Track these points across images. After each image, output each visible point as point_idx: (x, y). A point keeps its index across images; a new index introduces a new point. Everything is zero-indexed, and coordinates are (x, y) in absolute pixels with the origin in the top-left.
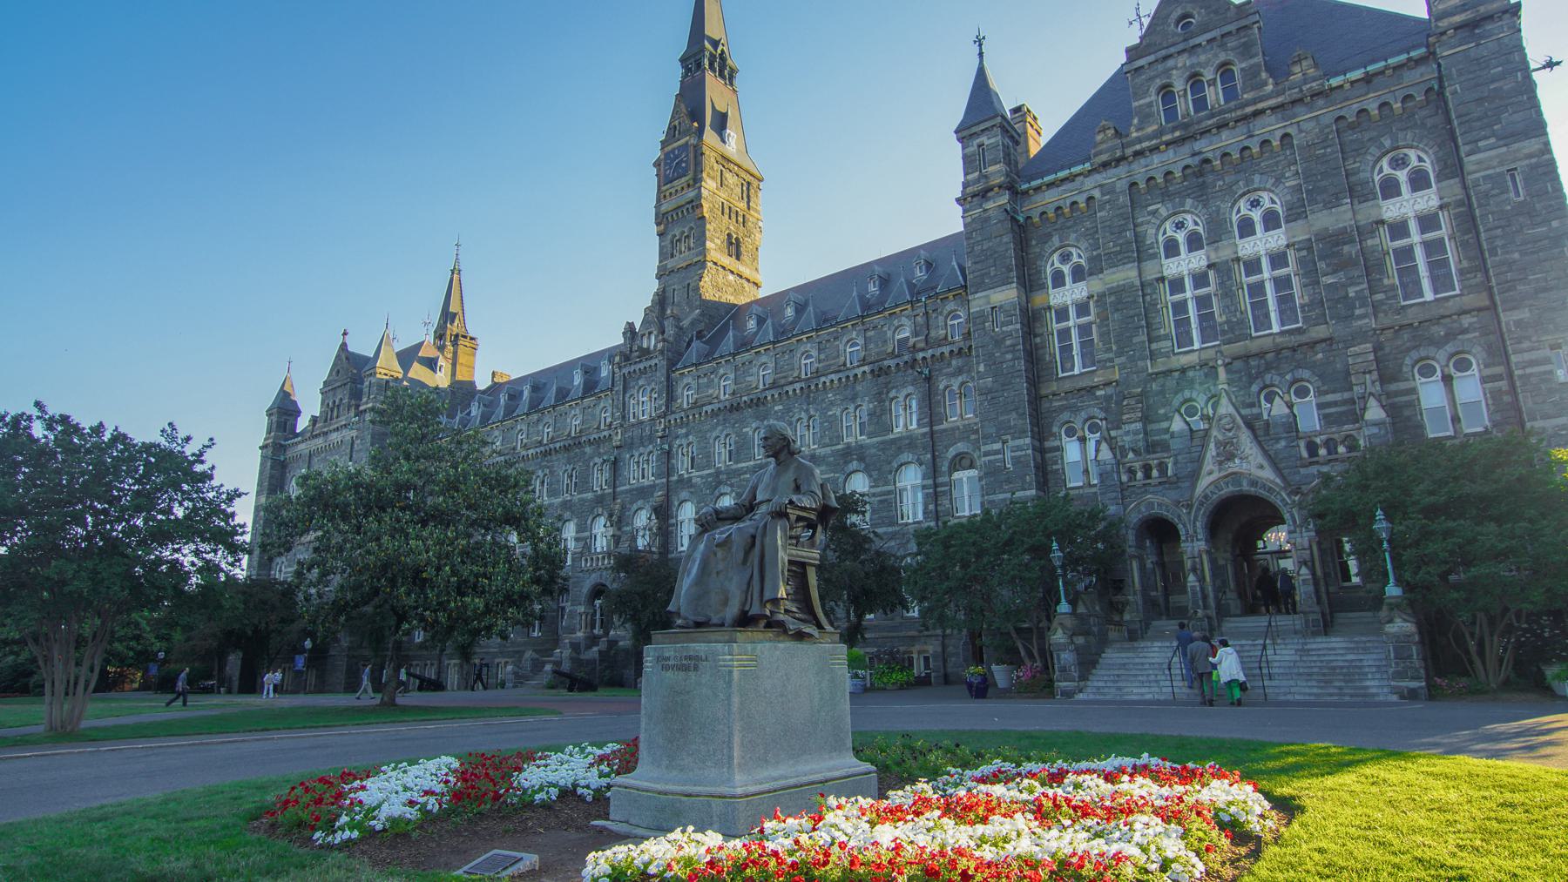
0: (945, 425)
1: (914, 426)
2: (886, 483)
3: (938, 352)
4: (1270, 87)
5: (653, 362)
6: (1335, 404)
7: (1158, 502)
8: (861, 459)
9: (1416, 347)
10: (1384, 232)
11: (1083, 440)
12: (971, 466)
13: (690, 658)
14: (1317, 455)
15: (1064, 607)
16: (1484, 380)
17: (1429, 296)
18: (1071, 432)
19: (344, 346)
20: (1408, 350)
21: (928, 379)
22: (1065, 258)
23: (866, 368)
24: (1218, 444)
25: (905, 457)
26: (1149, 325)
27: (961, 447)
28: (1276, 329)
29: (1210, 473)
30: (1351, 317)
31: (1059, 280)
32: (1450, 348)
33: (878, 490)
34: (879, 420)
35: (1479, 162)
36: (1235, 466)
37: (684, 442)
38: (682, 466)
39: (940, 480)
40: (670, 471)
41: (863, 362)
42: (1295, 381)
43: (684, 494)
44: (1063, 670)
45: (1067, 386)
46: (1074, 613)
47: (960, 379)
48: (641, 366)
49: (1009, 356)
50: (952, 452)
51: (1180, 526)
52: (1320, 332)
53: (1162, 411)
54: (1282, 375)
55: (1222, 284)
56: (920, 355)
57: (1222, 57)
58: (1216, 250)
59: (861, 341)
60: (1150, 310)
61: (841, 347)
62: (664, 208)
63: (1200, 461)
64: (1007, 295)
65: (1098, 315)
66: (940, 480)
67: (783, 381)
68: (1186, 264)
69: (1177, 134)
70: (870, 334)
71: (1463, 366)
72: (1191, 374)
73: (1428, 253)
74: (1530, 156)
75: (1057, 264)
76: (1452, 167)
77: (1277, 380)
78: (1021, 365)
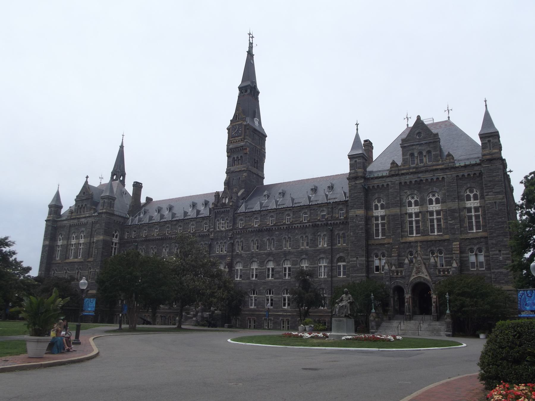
0: (336, 247)
1: (326, 246)
2: (315, 264)
3: (336, 222)
4: (440, 162)
5: (228, 209)
7: (400, 282)
8: (307, 254)
10: (466, 211)
12: (344, 261)
15: (373, 311)
16: (485, 256)
17: (475, 231)
18: (377, 256)
19: (86, 182)
21: (332, 230)
22: (379, 202)
23: (311, 224)
24: (416, 268)
25: (322, 256)
26: (402, 227)
27: (341, 254)
28: (436, 234)
29: (414, 276)
30: (454, 234)
31: (377, 208)
32: (477, 246)
33: (312, 266)
34: (314, 242)
35: (488, 198)
36: (421, 275)
37: (239, 240)
38: (238, 250)
39: (333, 265)
40: (233, 251)
41: (309, 222)
42: (439, 250)
43: (238, 260)
45: (377, 242)
46: (375, 312)
47: (342, 232)
48: (223, 210)
49: (360, 232)
50: (338, 256)
52: (447, 237)
54: (436, 248)
55: (422, 218)
56: (329, 222)
57: (429, 149)
58: (422, 207)
59: (309, 213)
60: (402, 223)
61: (301, 214)
62: (231, 146)
63: (411, 272)
64: (361, 212)
65: (387, 221)
66: (333, 265)
67: (279, 224)
68: (413, 209)
69: (414, 170)
70: (312, 211)
71: (480, 251)
72: (412, 244)
73: (476, 219)
74: (500, 199)
75: (376, 203)
76: (482, 197)
78: (364, 235)
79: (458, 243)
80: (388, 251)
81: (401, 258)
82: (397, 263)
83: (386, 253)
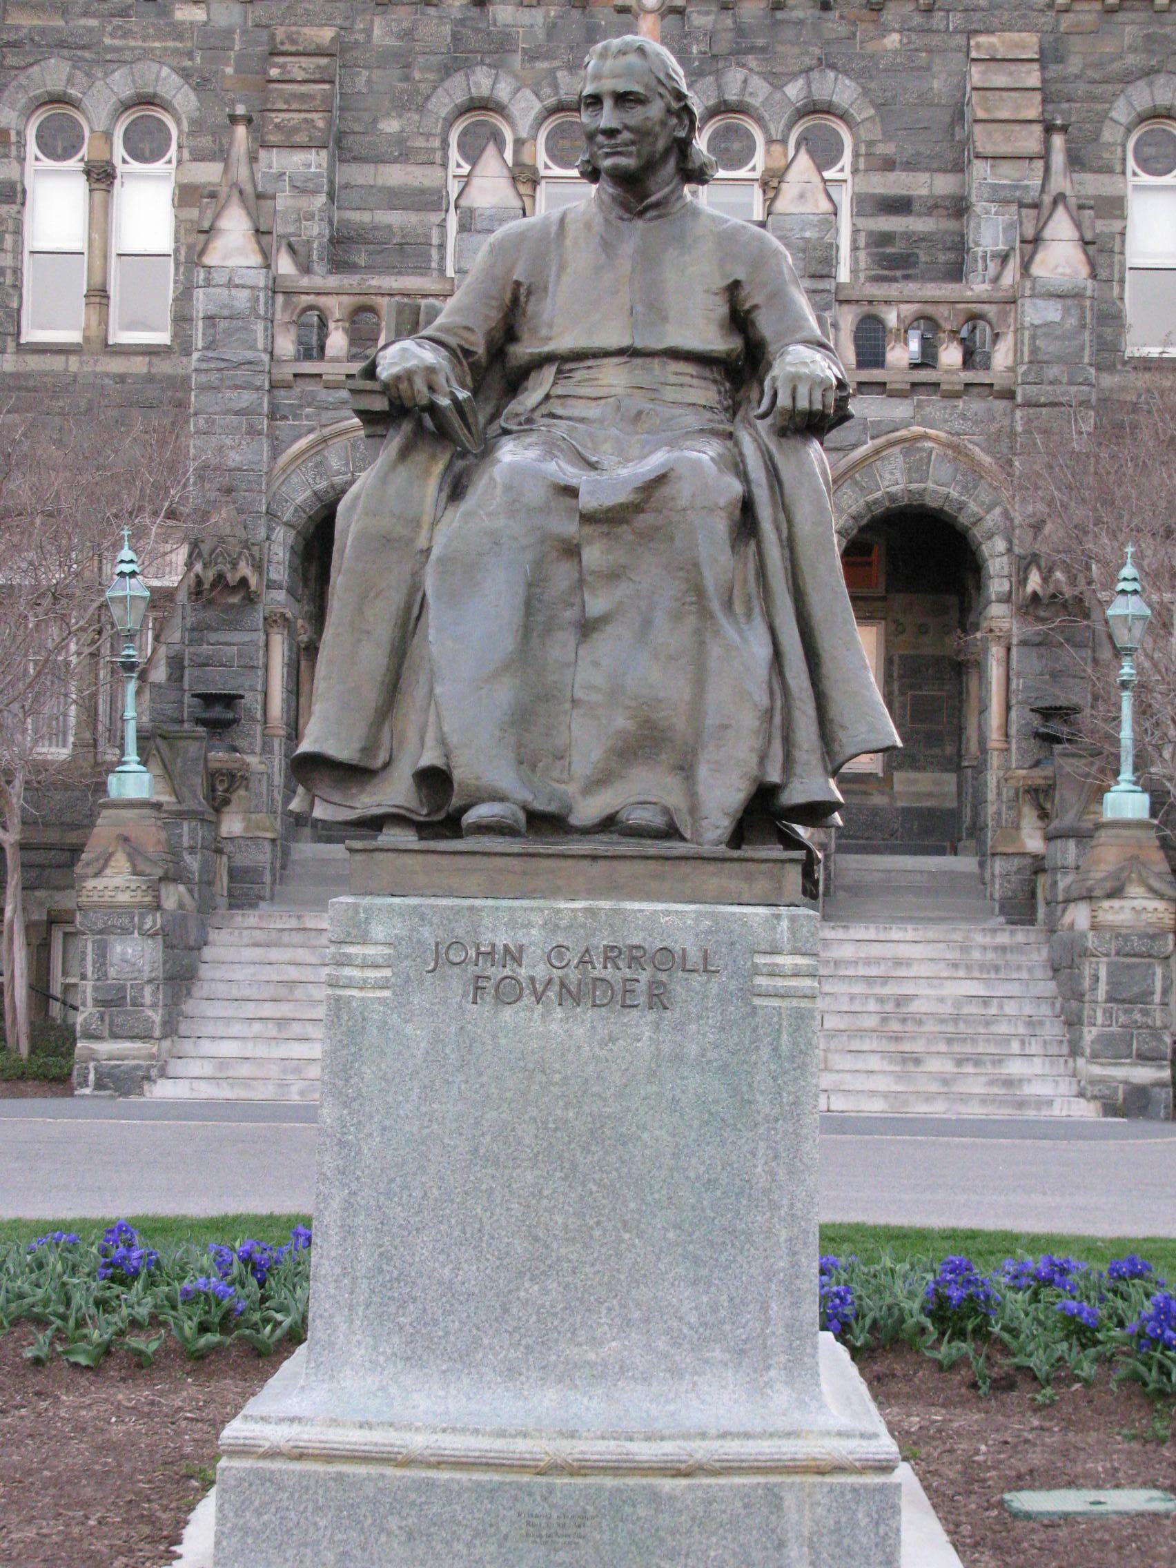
9: (1149, 73)
11: (101, 176)
13: (636, 956)
18: (60, 142)
20: (1127, 78)
42: (813, 108)
53: (391, 126)
54: (776, 80)
77: (759, 91)
79: (1029, 44)
80: (202, 84)
81: (360, 174)
82: (316, 230)
83: (185, 99)
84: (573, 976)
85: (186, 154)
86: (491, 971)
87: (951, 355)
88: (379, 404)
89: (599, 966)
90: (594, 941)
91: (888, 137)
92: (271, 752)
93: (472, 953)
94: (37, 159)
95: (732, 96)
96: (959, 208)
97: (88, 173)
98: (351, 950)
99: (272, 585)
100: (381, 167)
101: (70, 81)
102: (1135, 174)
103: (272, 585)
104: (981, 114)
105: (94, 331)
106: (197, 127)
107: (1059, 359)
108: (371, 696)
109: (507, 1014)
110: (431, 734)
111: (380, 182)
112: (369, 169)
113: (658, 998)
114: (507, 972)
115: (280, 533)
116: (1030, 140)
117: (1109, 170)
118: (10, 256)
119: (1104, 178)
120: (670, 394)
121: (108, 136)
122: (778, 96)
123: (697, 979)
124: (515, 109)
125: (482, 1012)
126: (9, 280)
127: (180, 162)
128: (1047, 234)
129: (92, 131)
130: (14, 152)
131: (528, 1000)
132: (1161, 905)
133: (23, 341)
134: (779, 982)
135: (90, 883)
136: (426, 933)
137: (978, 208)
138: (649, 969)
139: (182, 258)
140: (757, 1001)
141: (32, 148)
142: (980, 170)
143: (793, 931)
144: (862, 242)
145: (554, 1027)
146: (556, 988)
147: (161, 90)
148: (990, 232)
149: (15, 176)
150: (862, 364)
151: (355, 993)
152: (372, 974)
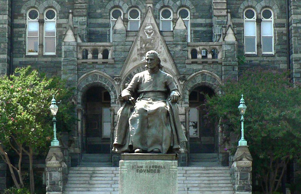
6: (201, 25)
11: (41, 22)
13: (156, 167)
14: (196, 57)
16: (276, 25)
18: (33, 15)
29: (135, 60)
42: (182, 6)
44: (53, 184)
46: (62, 148)
51: (112, 93)
53: (99, 11)
63: (129, 51)
71: (267, 15)
81: (93, 21)
82: (84, 32)
83: (58, 7)
84: (149, 169)
85: (58, 18)
86: (139, 169)
87: (210, 56)
88: (122, 100)
89: (152, 168)
90: (151, 165)
91: (197, 12)
92: (79, 136)
93: (137, 167)
94: (29, 19)
95: (166, 4)
96: (211, 25)
97: (39, 21)
98: (122, 167)
99: (78, 103)
100: (97, 19)
101: (35, 4)
102: (245, 18)
103: (78, 103)
104: (215, 8)
105: (40, 53)
106: (60, 12)
107: (230, 57)
108: (123, 136)
109: (141, 174)
110: (130, 142)
111: (97, 22)
112: (94, 20)
113: (159, 171)
114: (141, 169)
115: (79, 93)
116: (224, 13)
117: (240, 18)
118: (24, 38)
119: (240, 19)
120: (158, 96)
121: (43, 14)
122: (175, 4)
123: (163, 169)
124: (123, 7)
125: (138, 173)
126: (24, 43)
127: (57, 19)
128: (227, 33)
129: (40, 14)
130: (24, 18)
131: (143, 172)
132: (249, 162)
133: (26, 55)
134: (173, 169)
135: (48, 162)
136: (131, 165)
137: (215, 25)
138: (158, 168)
139: (58, 38)
140: (170, 172)
141: (28, 17)
142: (215, 19)
143: (174, 163)
144: (192, 32)
145: (147, 175)
146: (147, 171)
147: (53, 5)
148: (217, 30)
149: (25, 22)
150: (192, 58)
151: (123, 172)
152: (125, 170)
